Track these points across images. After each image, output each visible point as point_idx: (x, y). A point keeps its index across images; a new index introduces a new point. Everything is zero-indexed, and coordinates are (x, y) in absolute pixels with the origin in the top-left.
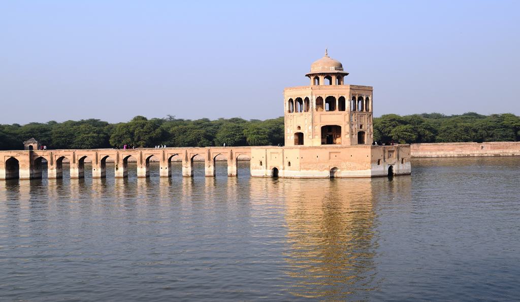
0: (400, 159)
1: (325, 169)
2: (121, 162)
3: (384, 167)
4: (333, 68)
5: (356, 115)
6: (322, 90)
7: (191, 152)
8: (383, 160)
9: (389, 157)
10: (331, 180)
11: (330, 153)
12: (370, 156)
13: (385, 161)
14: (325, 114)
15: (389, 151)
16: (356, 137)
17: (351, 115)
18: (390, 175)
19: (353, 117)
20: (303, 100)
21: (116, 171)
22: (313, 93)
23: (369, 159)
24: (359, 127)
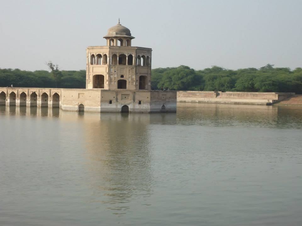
0: (137, 101)
1: (76, 105)
2: (9, 95)
3: (117, 105)
4: (115, 33)
5: (116, 68)
6: (94, 50)
7: (42, 91)
8: (115, 101)
9: (122, 99)
10: (122, 115)
11: (79, 94)
12: (100, 97)
13: (117, 101)
14: (95, 67)
15: (122, 94)
16: (116, 84)
17: (110, 67)
18: (125, 111)
19: (112, 70)
20: (102, 56)
21: (6, 102)
22: (89, 52)
23: (99, 99)
24: (120, 76)
